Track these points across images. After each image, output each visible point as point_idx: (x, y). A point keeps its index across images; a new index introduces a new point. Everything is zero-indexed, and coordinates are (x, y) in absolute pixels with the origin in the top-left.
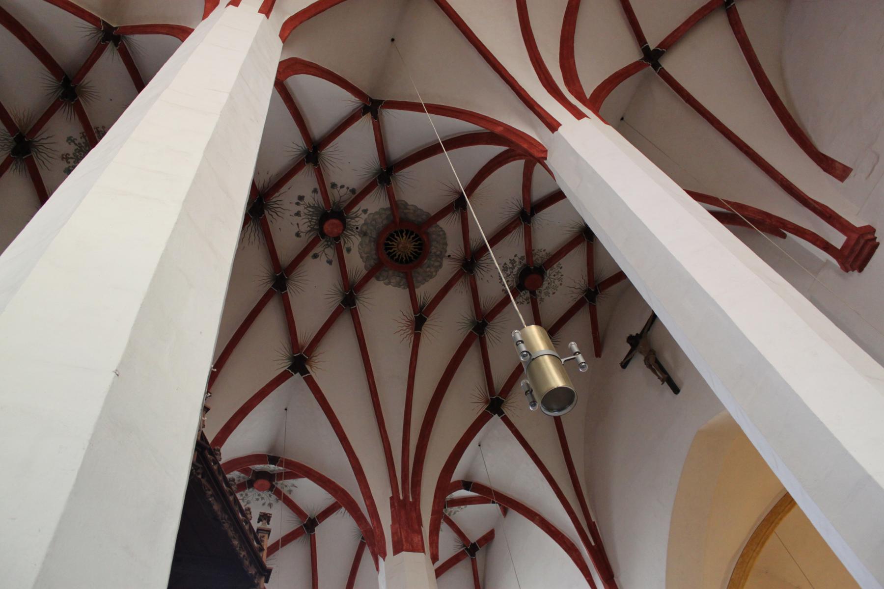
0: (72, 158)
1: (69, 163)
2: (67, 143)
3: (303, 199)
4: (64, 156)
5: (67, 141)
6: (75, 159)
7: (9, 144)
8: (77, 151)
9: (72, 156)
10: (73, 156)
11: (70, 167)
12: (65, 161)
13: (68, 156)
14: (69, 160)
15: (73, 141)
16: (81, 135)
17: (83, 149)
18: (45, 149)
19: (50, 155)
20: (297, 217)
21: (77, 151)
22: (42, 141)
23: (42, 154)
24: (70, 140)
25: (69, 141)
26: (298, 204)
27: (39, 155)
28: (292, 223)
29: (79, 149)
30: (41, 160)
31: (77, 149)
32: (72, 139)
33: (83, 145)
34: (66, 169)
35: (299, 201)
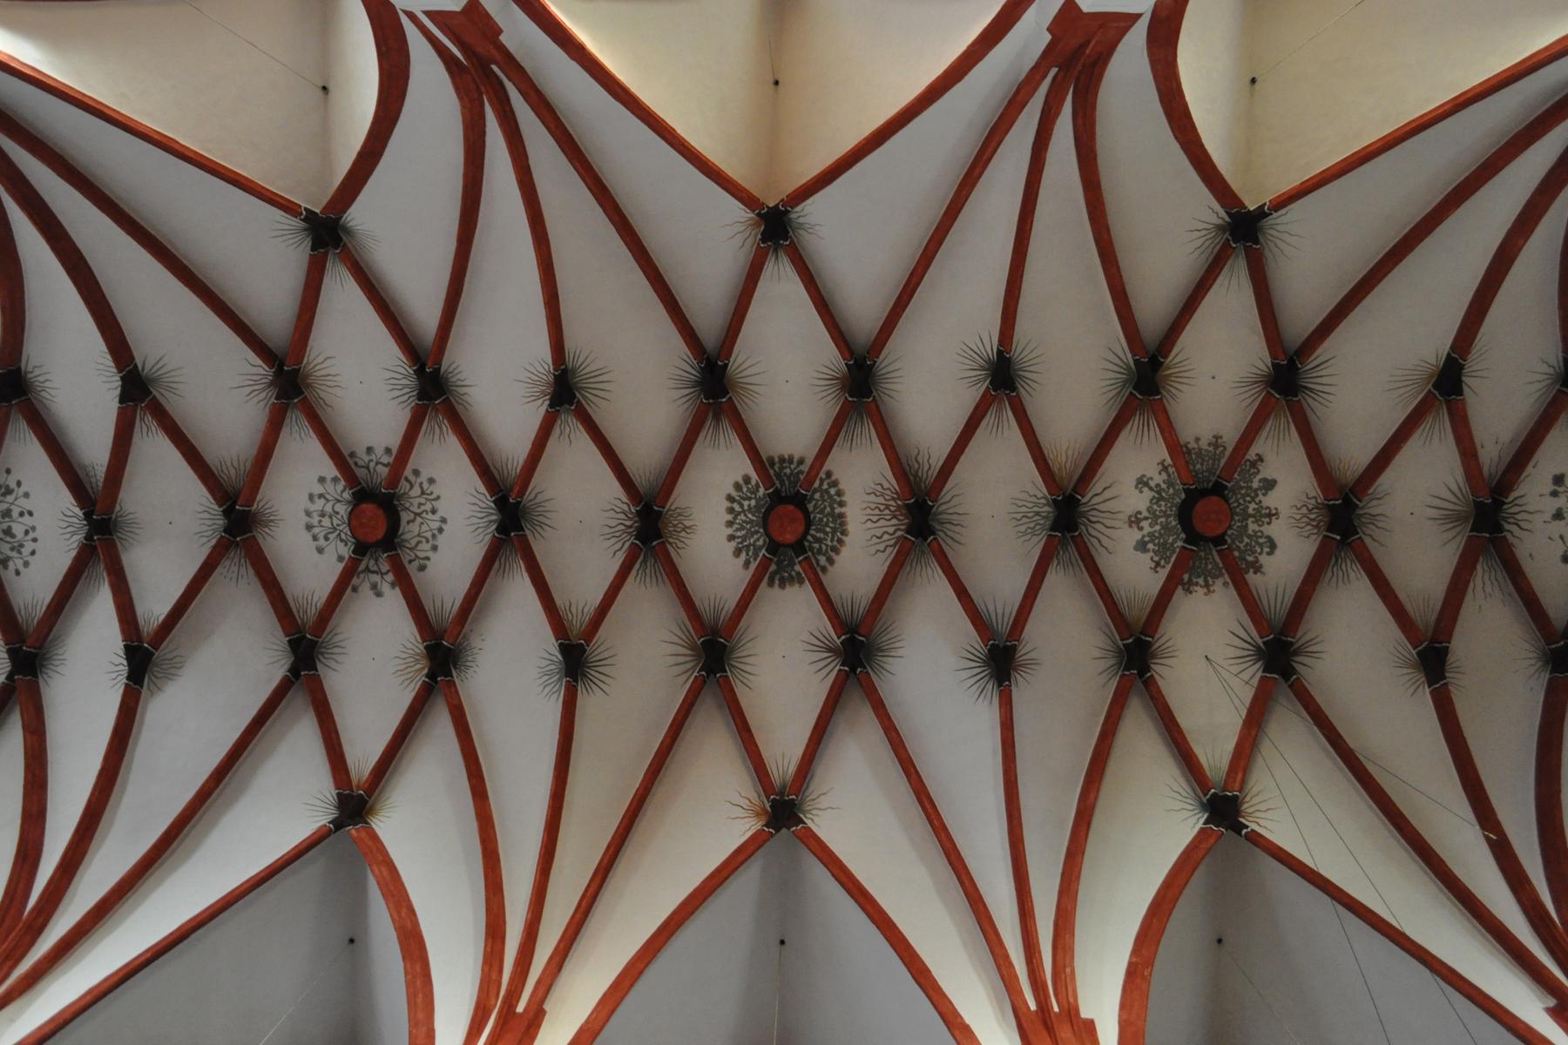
0: (1146, 518)
1: (1141, 529)
2: (1137, 491)
3: (1563, 481)
4: (1133, 519)
5: (1136, 487)
6: (1151, 518)
7: (1042, 522)
8: (1155, 501)
9: (1145, 514)
10: (1147, 515)
11: (1144, 536)
12: (1136, 529)
13: (1139, 516)
14: (1145, 524)
15: (1146, 484)
16: (1160, 467)
17: (1164, 494)
18: (1101, 514)
19: (1108, 523)
20: (1557, 522)
21: (1155, 501)
22: (1093, 501)
23: (1097, 526)
24: (1142, 483)
25: (1140, 486)
26: (1554, 494)
27: (1090, 529)
28: (1550, 538)
29: (1157, 496)
30: (1097, 538)
31: (1154, 497)
32: (1145, 479)
33: (1164, 486)
34: (1138, 542)
35: (1556, 488)
